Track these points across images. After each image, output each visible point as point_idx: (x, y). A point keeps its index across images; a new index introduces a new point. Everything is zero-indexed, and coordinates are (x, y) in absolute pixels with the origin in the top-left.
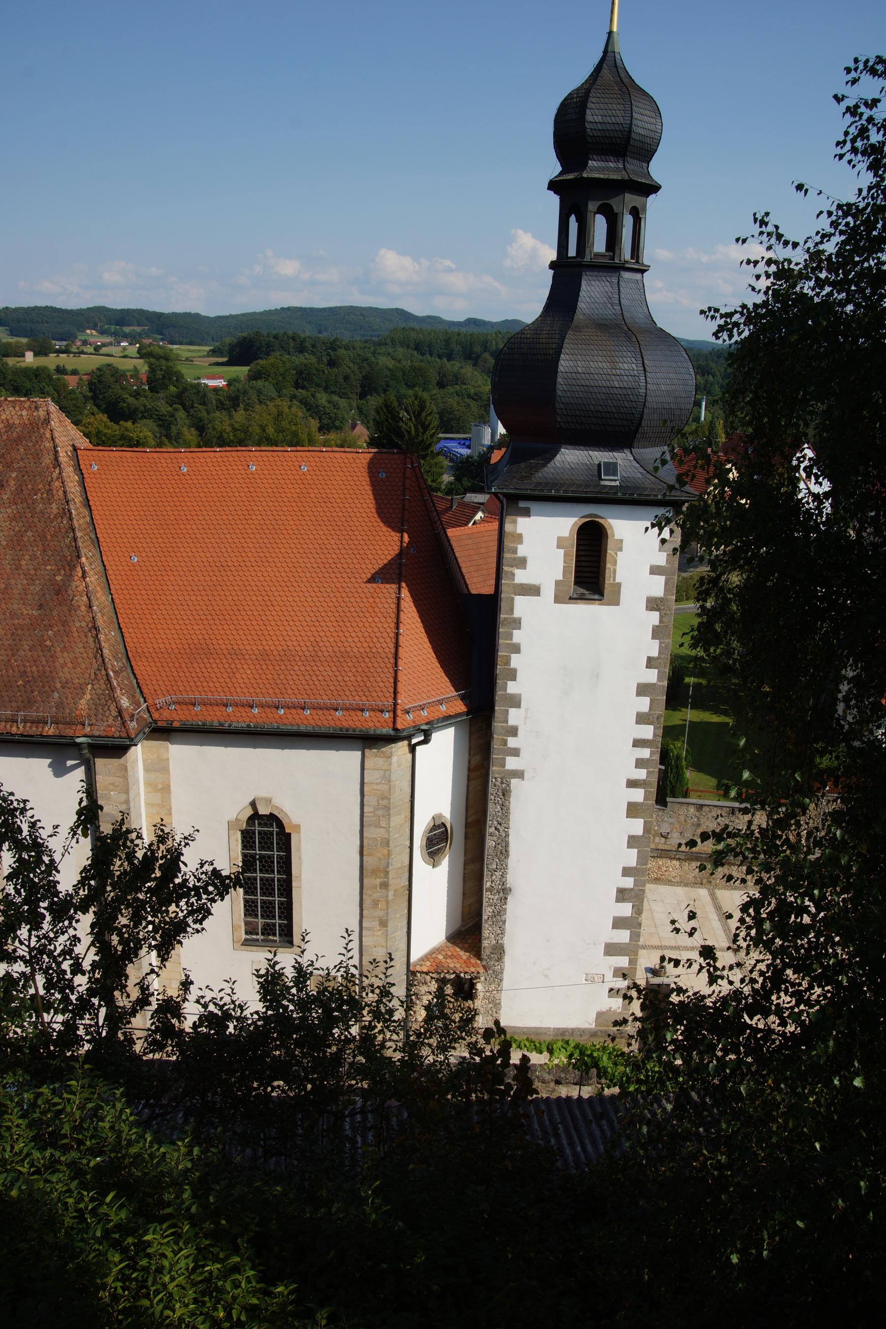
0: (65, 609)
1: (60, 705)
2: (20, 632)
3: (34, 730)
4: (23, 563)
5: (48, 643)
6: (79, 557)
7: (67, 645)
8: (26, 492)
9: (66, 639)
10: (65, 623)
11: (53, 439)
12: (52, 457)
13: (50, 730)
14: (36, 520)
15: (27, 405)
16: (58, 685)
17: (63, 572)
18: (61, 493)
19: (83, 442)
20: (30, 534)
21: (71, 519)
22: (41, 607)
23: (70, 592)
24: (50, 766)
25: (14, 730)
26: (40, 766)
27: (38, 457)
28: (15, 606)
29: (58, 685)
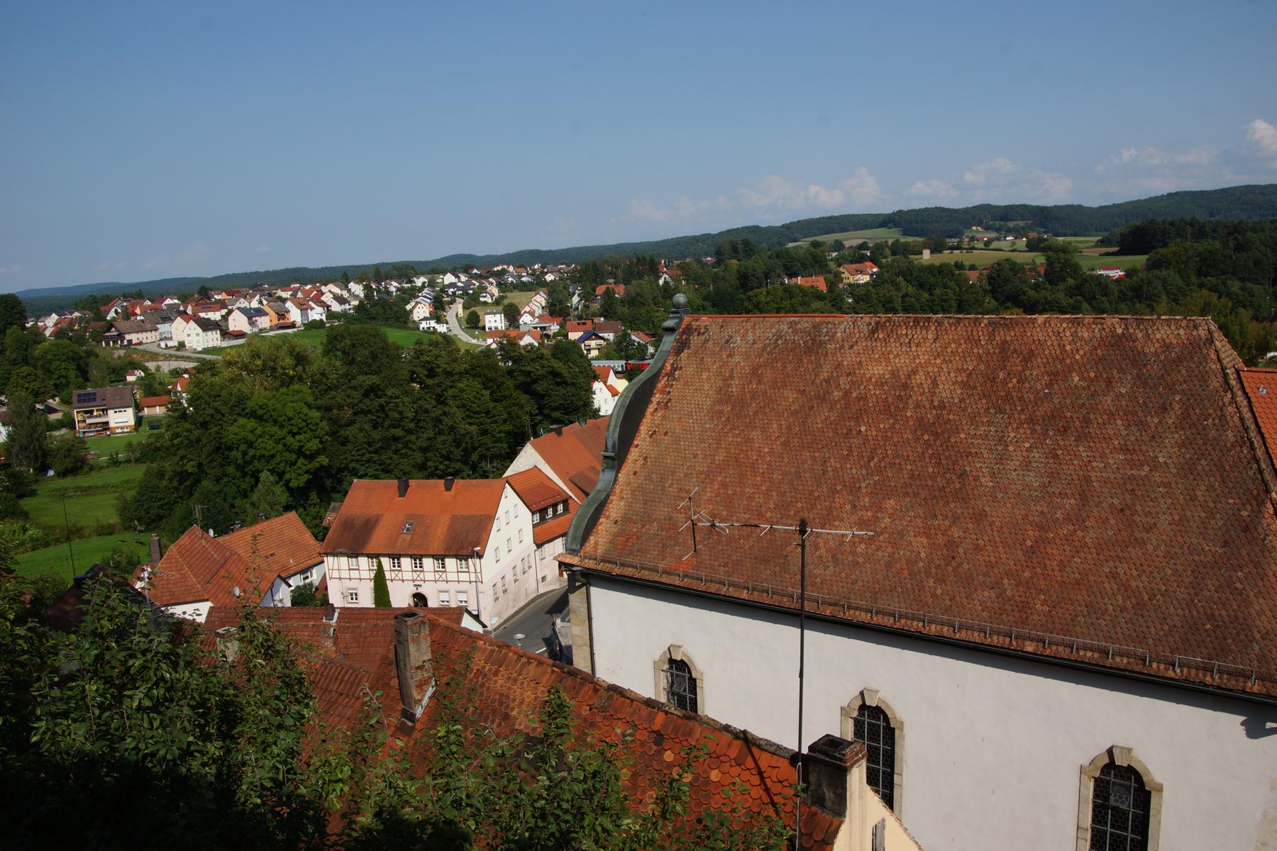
0: (1257, 549)
1: (1262, 659)
2: (1201, 569)
3: (1232, 684)
4: (1199, 493)
5: (1238, 585)
6: (1268, 491)
7: (1263, 590)
8: (1194, 417)
9: (1260, 583)
10: (1257, 565)
11: (1219, 360)
12: (1221, 380)
13: (1255, 687)
14: (1210, 448)
15: (1184, 324)
16: (1258, 636)
17: (1249, 507)
18: (1236, 419)
19: (1240, 365)
20: (1203, 462)
21: (1252, 448)
22: (1225, 544)
23: (1260, 530)
24: (1243, 724)
25: (1208, 679)
26: (1231, 723)
27: (1204, 378)
28: (1194, 541)
29: (1258, 636)
